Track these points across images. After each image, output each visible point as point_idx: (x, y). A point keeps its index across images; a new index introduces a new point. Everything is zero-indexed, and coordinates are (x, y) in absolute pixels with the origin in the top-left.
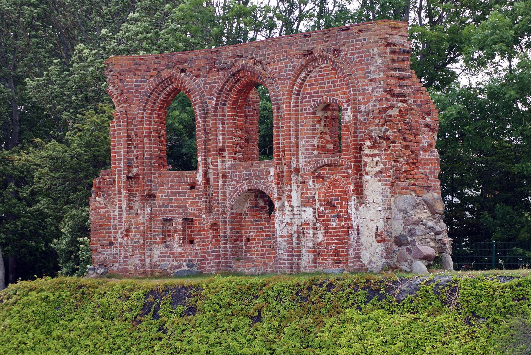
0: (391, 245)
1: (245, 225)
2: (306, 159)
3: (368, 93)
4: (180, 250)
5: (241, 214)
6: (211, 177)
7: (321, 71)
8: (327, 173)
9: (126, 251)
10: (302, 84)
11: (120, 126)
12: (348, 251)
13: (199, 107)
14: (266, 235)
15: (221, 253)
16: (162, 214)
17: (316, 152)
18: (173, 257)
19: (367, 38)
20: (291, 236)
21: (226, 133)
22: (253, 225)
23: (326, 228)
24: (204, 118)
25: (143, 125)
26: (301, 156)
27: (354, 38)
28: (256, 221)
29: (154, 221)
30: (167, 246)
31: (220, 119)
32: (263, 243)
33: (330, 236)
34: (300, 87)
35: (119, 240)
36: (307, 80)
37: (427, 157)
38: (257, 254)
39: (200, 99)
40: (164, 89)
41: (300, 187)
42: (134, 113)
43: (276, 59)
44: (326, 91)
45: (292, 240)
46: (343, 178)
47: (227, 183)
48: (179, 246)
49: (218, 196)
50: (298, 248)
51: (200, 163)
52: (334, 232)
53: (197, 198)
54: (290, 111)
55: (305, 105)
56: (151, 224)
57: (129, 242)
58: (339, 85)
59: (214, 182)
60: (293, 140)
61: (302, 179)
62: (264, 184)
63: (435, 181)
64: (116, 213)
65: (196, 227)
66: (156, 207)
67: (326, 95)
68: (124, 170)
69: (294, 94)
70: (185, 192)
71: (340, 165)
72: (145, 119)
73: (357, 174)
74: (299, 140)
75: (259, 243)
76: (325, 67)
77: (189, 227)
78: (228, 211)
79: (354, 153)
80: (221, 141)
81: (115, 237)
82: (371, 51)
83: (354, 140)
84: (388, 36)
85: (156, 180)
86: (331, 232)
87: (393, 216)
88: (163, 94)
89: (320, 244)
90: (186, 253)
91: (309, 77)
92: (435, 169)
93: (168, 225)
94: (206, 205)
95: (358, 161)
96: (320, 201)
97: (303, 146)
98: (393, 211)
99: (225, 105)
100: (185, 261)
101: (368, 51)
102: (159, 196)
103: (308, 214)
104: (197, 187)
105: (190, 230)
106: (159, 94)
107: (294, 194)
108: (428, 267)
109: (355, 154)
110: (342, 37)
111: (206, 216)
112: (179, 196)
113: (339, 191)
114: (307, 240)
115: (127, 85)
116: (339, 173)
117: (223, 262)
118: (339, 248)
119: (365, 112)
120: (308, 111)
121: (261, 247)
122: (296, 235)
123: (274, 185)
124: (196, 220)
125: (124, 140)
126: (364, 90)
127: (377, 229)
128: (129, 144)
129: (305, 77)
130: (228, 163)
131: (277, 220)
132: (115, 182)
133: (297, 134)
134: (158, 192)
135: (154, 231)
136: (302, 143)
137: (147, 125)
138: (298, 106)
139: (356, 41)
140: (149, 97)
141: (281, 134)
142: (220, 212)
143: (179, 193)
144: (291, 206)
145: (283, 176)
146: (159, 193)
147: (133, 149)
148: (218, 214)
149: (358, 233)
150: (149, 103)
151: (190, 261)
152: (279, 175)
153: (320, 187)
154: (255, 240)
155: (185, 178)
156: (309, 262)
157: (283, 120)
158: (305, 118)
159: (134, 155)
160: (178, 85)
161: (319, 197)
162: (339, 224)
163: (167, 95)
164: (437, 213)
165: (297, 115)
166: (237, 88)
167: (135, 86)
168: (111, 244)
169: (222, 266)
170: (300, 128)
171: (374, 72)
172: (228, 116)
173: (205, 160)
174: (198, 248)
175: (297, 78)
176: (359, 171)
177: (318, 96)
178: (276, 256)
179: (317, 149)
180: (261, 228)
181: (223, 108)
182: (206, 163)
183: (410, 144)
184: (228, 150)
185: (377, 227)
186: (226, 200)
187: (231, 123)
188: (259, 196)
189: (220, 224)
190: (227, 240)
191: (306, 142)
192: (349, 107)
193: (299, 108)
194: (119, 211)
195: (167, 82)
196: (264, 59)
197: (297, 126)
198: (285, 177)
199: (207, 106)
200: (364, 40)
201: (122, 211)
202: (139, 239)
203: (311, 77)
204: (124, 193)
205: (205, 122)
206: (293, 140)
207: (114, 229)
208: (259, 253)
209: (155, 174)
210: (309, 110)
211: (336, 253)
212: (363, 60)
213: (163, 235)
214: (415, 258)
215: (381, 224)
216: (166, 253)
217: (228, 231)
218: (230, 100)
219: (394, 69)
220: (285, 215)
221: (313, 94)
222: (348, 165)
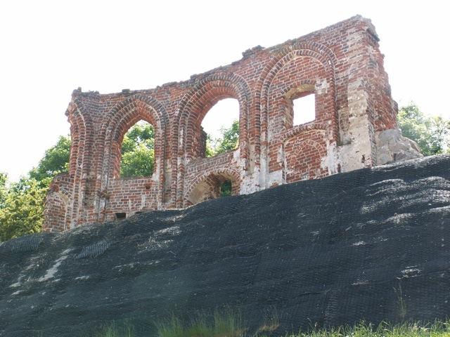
10: (272, 77)
46: (314, 141)
51: (159, 165)
64: (72, 206)
78: (185, 199)
107: (263, 163)
113: (311, 153)
127: (364, 158)
129: (276, 71)
132: (73, 181)
175: (268, 71)
177: (289, 83)
215: (368, 153)
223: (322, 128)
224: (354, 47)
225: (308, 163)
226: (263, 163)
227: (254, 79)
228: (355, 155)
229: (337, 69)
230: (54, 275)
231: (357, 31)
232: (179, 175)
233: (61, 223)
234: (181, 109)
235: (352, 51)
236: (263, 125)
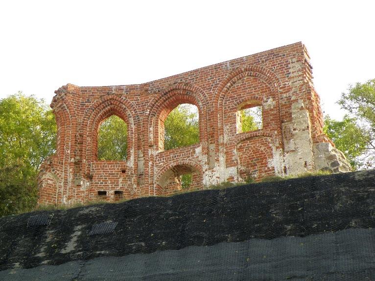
10: (227, 91)
19: (285, 54)
26: (225, 136)
40: (104, 108)
70: (118, 174)
78: (155, 183)
88: (102, 112)
103: (233, 171)
126: (286, 84)
127: (306, 164)
129: (230, 87)
134: (94, 174)
137: (89, 129)
143: (112, 174)
150: (92, 115)
159: (78, 148)
171: (293, 73)
191: (230, 126)
215: (310, 160)
223: (268, 136)
224: (295, 74)
226: (222, 159)
227: (212, 91)
228: (299, 161)
229: (281, 90)
230: (75, 247)
231: (297, 61)
233: (54, 198)
234: (151, 110)
235: (293, 77)
236: (220, 129)
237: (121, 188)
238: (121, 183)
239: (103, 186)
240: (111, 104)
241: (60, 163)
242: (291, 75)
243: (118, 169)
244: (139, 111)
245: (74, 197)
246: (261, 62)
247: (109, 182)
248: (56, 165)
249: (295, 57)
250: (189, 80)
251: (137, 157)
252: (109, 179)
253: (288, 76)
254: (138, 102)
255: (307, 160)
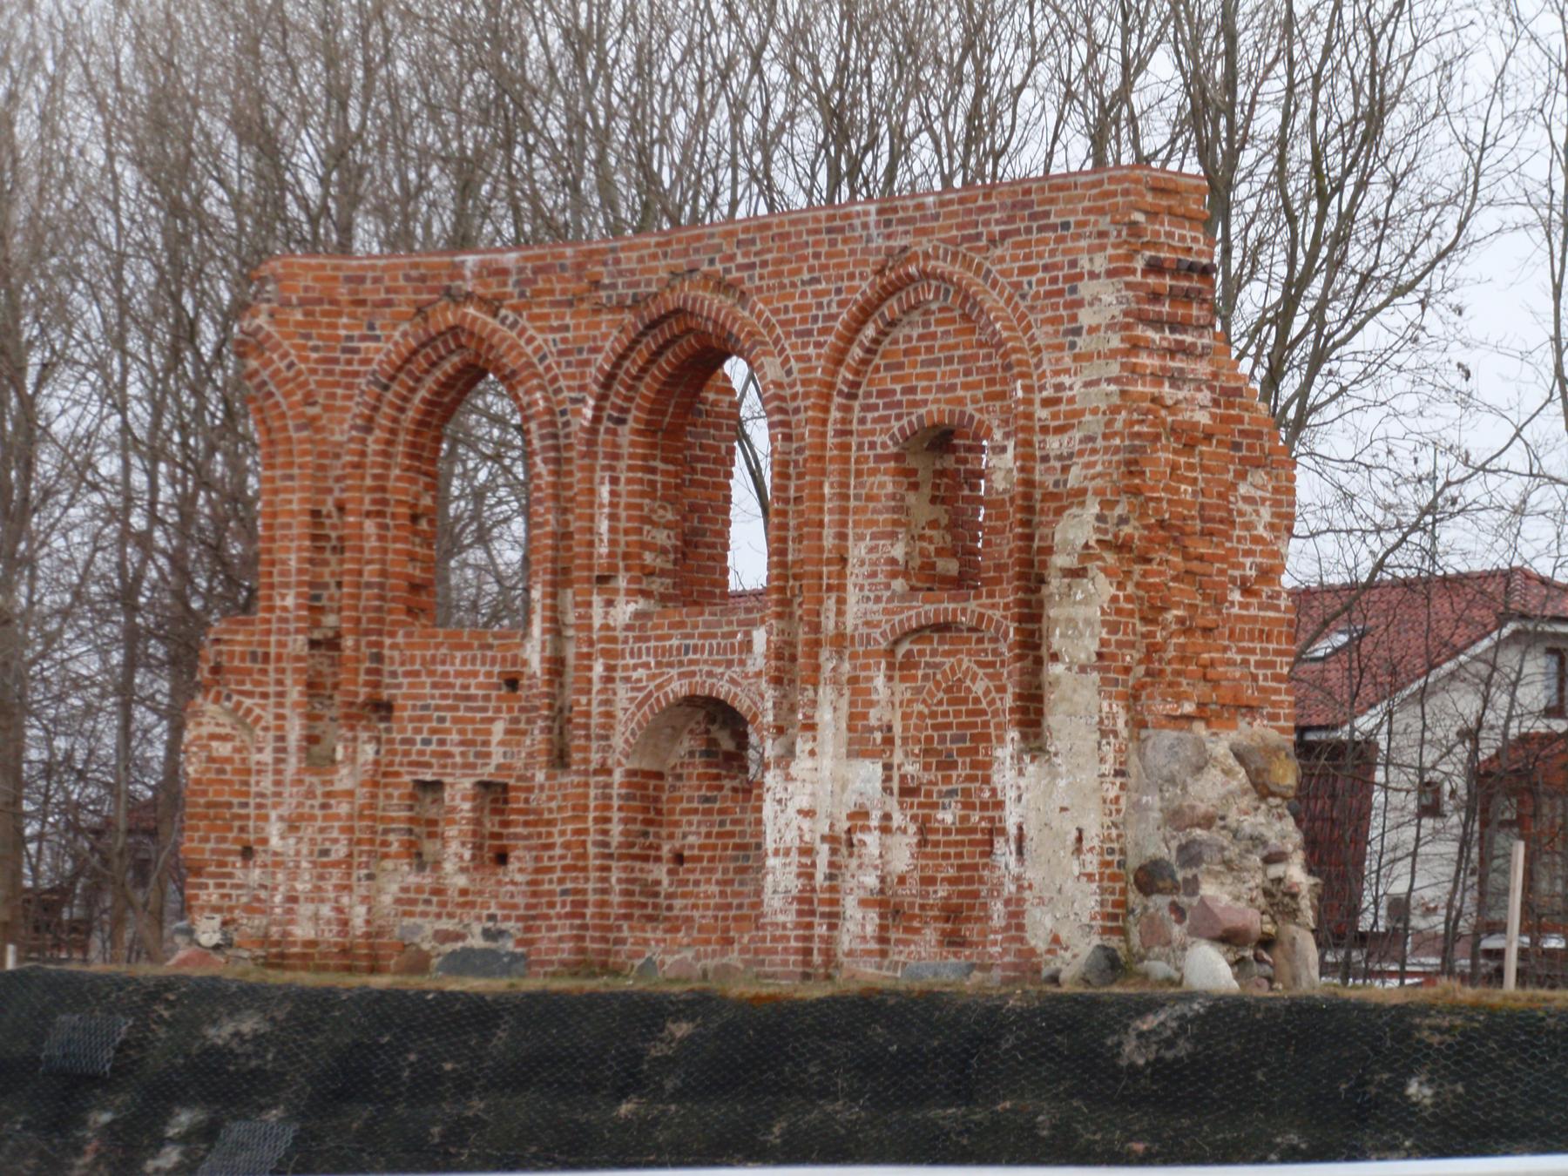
0: (1124, 892)
1: (671, 812)
2: (870, 605)
3: (1071, 400)
4: (462, 881)
5: (659, 776)
6: (570, 652)
7: (926, 324)
8: (934, 653)
9: (293, 875)
10: (865, 362)
11: (291, 478)
12: (984, 906)
13: (541, 426)
14: (737, 847)
15: (591, 898)
16: (411, 764)
17: (899, 584)
18: (443, 904)
19: (1072, 219)
20: (807, 851)
21: (623, 514)
22: (695, 811)
23: (922, 831)
24: (557, 461)
25: (363, 478)
26: (852, 596)
27: (1033, 217)
28: (707, 799)
29: (386, 785)
30: (421, 867)
31: (604, 468)
32: (725, 871)
33: (934, 856)
34: (857, 373)
35: (275, 842)
36: (881, 349)
37: (1253, 612)
38: (706, 907)
39: (546, 399)
40: (434, 364)
41: (846, 692)
42: (337, 437)
43: (786, 281)
44: (941, 388)
45: (814, 865)
46: (981, 672)
47: (619, 674)
48: (463, 870)
49: (588, 714)
50: (833, 889)
51: (538, 607)
52: (947, 844)
53: (523, 717)
54: (823, 446)
55: (872, 432)
56: (374, 796)
57: (305, 849)
58: (980, 370)
59: (577, 668)
60: (829, 541)
61: (854, 668)
62: (732, 681)
63: (1277, 691)
64: (267, 756)
65: (520, 812)
66: (391, 741)
67: (937, 401)
68: (299, 619)
69: (840, 393)
71: (970, 630)
72: (370, 459)
73: (1020, 658)
74: (850, 543)
75: (712, 871)
76: (941, 310)
77: (495, 811)
78: (619, 764)
79: (1017, 589)
80: (605, 537)
81: (258, 830)
82: (1084, 263)
83: (1020, 550)
84: (1139, 217)
85: (396, 654)
86: (936, 844)
87: (1135, 796)
88: (429, 382)
89: (902, 880)
90: (481, 893)
91: (887, 341)
92: (1278, 653)
93: (429, 799)
94: (550, 741)
95: (1031, 616)
96: (905, 740)
97: (862, 563)
98: (1132, 782)
99: (622, 421)
100: (478, 918)
101: (1073, 264)
102: (404, 708)
104: (524, 682)
105: (497, 818)
106: (418, 380)
107: (825, 716)
108: (1239, 964)
109: (1020, 595)
110: (997, 215)
111: (548, 777)
112: (468, 709)
113: (970, 713)
114: (860, 866)
115: (315, 349)
116: (969, 653)
117: (596, 927)
118: (961, 894)
119: (1060, 458)
120: (879, 451)
121: (718, 883)
122: (824, 849)
123: (764, 685)
124: (516, 789)
125: (299, 526)
126: (1059, 387)
127: (1080, 839)
128: (315, 538)
129: (876, 341)
130: (624, 611)
131: (768, 797)
133: (844, 524)
135: (383, 819)
136: (858, 551)
138: (850, 433)
139: (1041, 229)
140: (386, 388)
141: (792, 523)
142: (593, 766)
144: (812, 753)
145: (793, 658)
146: (406, 697)
147: (328, 555)
148: (586, 773)
149: (1020, 851)
150: (386, 409)
151: (492, 917)
152: (783, 653)
153: (908, 695)
154: (699, 859)
155: (489, 653)
156: (864, 939)
157: (800, 476)
158: (873, 472)
159: (333, 574)
160: (478, 355)
161: (905, 729)
162: (964, 819)
163: (442, 385)
164: (1273, 794)
165: (846, 460)
166: (662, 370)
167: (345, 350)
168: (247, 853)
169: (593, 940)
170: (852, 503)
171: (1092, 330)
172: (631, 456)
173: (554, 596)
174: (519, 878)
175: (850, 341)
176: (1032, 648)
177: (914, 404)
178: (762, 915)
179: (906, 574)
180: (722, 823)
181: (614, 433)
182: (554, 608)
183: (1195, 565)
184: (628, 568)
185: (1080, 831)
186: (612, 727)
187: (641, 481)
188: (720, 718)
189: (592, 804)
190: (610, 856)
192: (1011, 444)
193: (854, 441)
194: (277, 750)
195: (445, 343)
196: (751, 278)
197: (846, 497)
198: (801, 661)
199: (567, 424)
200: (1066, 226)
201: (284, 750)
202: (335, 841)
203: (895, 342)
204: (295, 693)
205: (556, 473)
206: (829, 541)
207: (260, 806)
208: (712, 902)
209: (392, 634)
210: (884, 445)
211: (952, 913)
212: (1060, 293)
213: (410, 831)
214: (1195, 932)
216: (419, 889)
217: (616, 829)
218: (639, 408)
219: (1157, 323)
220: (788, 778)
221: (898, 397)
222: (997, 630)
225: (961, 752)
231: (1111, 273)
232: (598, 668)
233: (240, 817)
237: (499, 767)
238: (502, 743)
239: (434, 754)
240: (460, 346)
241: (254, 656)
242: (1083, 343)
243: (489, 674)
244: (570, 388)
245: (312, 818)
246: (983, 242)
247: (455, 737)
248: (237, 671)
249: (1103, 248)
250: (740, 268)
251: (556, 627)
252: (455, 720)
253: (1073, 345)
254: (565, 340)
255: (1083, 823)
